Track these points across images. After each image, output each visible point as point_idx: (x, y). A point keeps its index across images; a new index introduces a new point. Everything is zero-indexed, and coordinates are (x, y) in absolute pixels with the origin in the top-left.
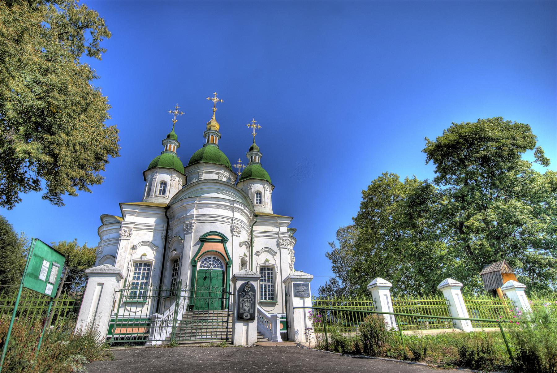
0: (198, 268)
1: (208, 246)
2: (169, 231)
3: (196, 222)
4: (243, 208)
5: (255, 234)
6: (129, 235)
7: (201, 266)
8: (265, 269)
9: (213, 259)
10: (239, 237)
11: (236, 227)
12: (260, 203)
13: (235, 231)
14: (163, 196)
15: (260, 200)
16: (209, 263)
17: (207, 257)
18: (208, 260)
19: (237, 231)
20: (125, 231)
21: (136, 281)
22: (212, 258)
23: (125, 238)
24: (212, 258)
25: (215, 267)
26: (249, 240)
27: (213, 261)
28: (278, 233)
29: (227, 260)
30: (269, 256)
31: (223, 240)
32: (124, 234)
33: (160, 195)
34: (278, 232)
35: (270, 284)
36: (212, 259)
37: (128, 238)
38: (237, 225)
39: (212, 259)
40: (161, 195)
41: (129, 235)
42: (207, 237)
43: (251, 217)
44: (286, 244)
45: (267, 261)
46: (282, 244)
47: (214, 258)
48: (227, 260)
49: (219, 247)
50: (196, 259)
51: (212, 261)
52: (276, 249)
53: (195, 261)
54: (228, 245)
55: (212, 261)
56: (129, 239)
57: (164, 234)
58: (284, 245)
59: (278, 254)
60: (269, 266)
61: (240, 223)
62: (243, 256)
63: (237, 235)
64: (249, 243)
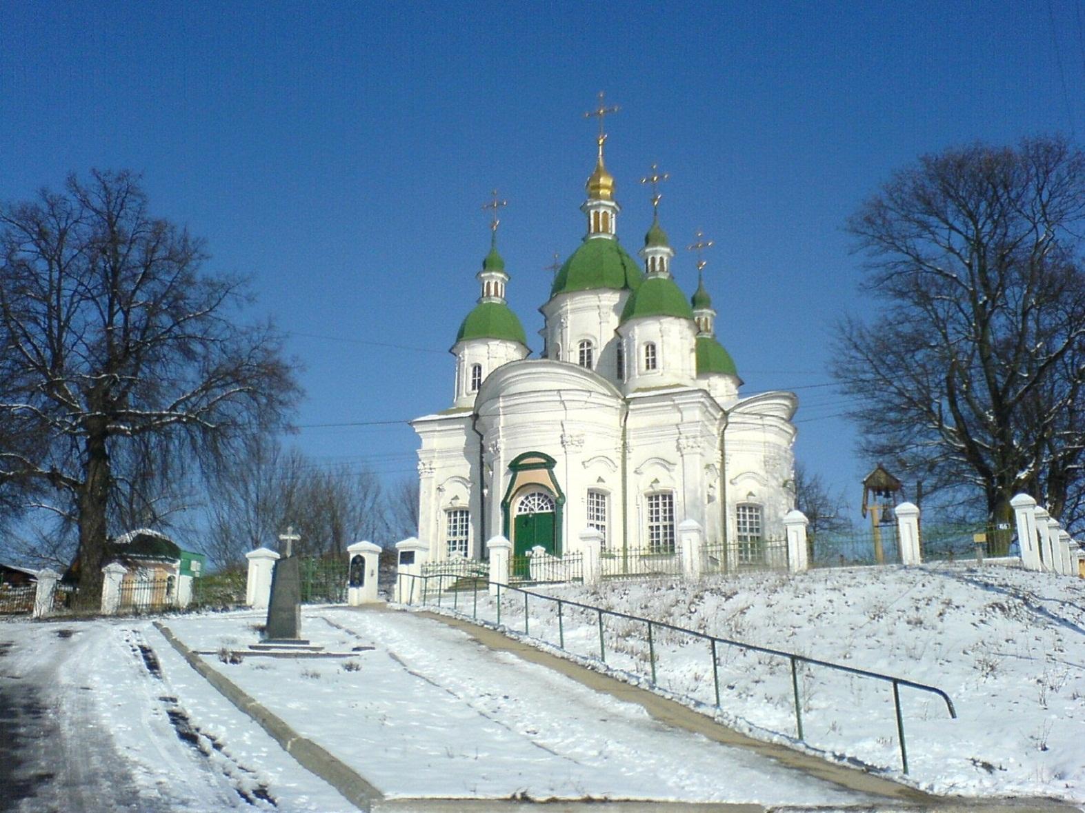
0: (515, 512)
1: (524, 477)
7: (520, 510)
8: (657, 498)
15: (654, 360)
21: (452, 538)
25: (542, 508)
27: (539, 500)
30: (660, 472)
31: (549, 463)
35: (667, 523)
39: (536, 498)
42: (520, 463)
47: (540, 495)
49: (541, 476)
50: (508, 500)
52: (673, 456)
54: (554, 470)
59: (678, 468)
60: (662, 491)
62: (595, 483)
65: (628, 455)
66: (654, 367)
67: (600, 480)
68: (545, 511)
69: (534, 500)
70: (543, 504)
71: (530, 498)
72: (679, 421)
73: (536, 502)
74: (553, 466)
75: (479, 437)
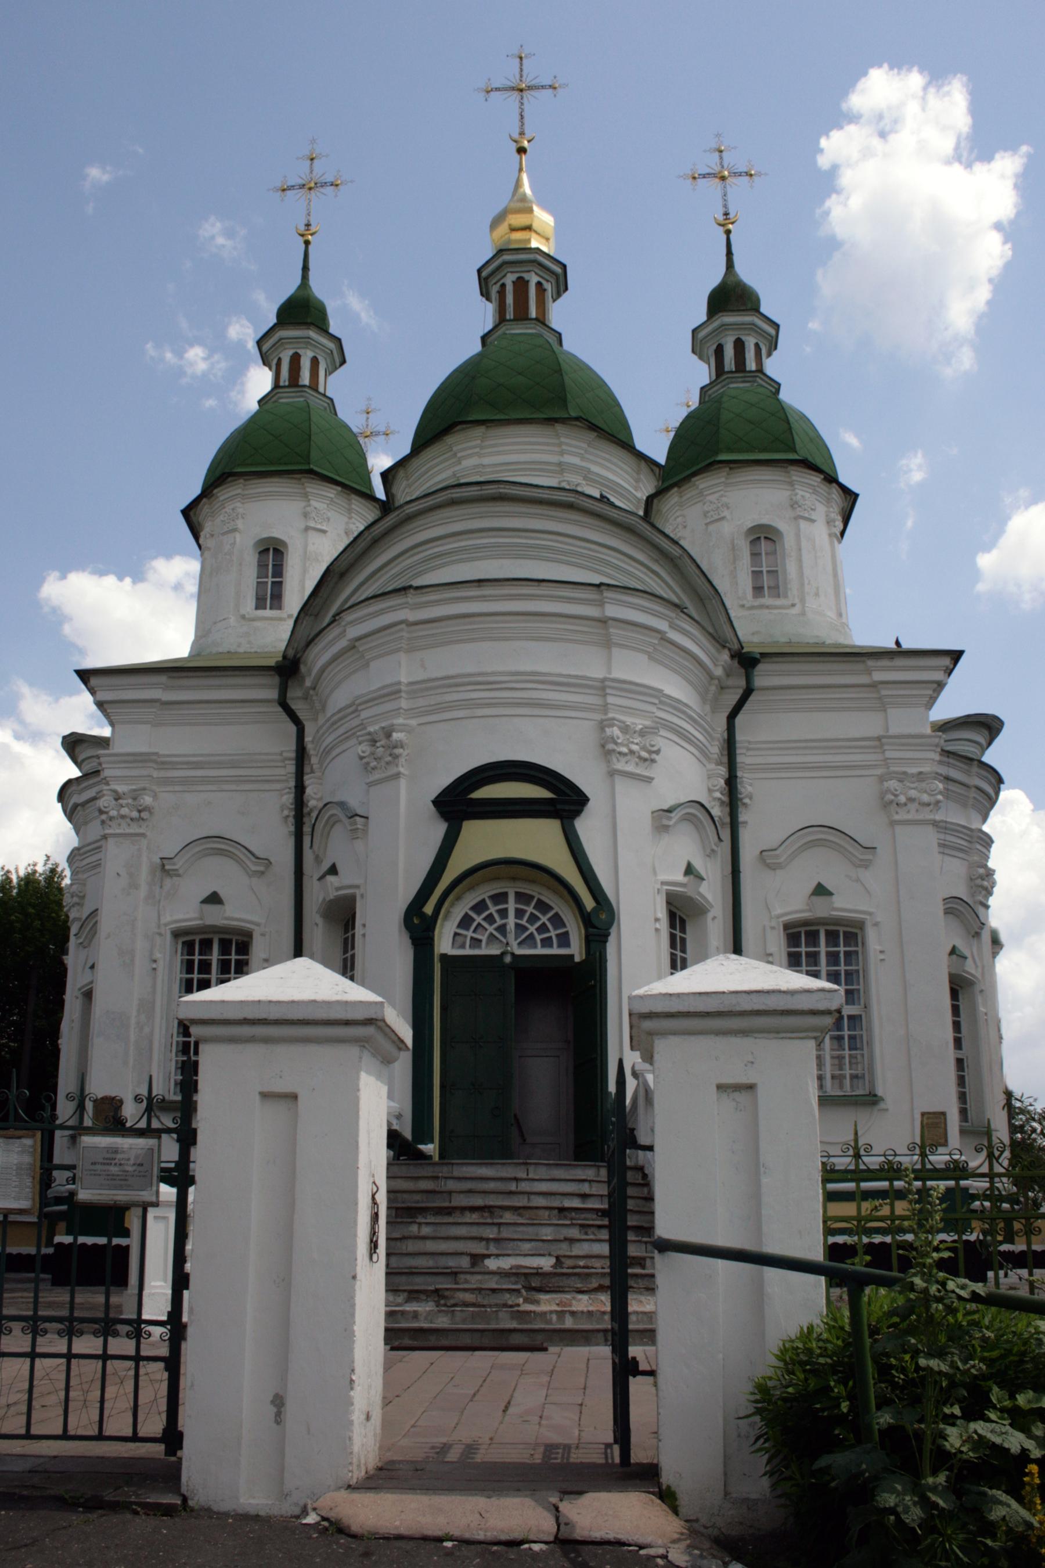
2: (308, 780)
3: (413, 722)
4: (662, 625)
5: (748, 760)
6: (135, 814)
8: (812, 937)
9: (518, 901)
10: (649, 780)
11: (625, 729)
12: (776, 590)
13: (625, 750)
14: (275, 613)
16: (499, 922)
17: (484, 892)
18: (493, 909)
19: (635, 747)
20: (118, 797)
22: (511, 898)
23: (124, 828)
24: (511, 898)
26: (718, 795)
27: (519, 913)
28: (879, 742)
29: (589, 903)
32: (113, 813)
33: (261, 613)
34: (879, 739)
36: (511, 906)
37: (134, 829)
38: (629, 720)
39: (511, 906)
40: (268, 613)
41: (135, 814)
43: (719, 672)
44: (925, 798)
45: (821, 890)
46: (902, 799)
47: (521, 897)
48: (589, 903)
50: (429, 909)
51: (511, 913)
53: (423, 916)
54: (587, 827)
55: (511, 913)
56: (141, 831)
57: (289, 799)
58: (912, 807)
60: (838, 922)
61: (653, 709)
62: (679, 877)
63: (638, 771)
64: (716, 812)
65: (742, 817)
66: (776, 590)
67: (689, 870)
68: (540, 951)
69: (504, 913)
70: (532, 929)
71: (493, 909)
72: (880, 732)
73: (511, 921)
74: (578, 813)
75: (293, 729)
